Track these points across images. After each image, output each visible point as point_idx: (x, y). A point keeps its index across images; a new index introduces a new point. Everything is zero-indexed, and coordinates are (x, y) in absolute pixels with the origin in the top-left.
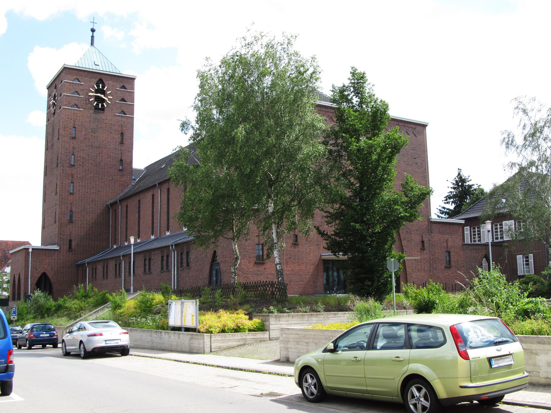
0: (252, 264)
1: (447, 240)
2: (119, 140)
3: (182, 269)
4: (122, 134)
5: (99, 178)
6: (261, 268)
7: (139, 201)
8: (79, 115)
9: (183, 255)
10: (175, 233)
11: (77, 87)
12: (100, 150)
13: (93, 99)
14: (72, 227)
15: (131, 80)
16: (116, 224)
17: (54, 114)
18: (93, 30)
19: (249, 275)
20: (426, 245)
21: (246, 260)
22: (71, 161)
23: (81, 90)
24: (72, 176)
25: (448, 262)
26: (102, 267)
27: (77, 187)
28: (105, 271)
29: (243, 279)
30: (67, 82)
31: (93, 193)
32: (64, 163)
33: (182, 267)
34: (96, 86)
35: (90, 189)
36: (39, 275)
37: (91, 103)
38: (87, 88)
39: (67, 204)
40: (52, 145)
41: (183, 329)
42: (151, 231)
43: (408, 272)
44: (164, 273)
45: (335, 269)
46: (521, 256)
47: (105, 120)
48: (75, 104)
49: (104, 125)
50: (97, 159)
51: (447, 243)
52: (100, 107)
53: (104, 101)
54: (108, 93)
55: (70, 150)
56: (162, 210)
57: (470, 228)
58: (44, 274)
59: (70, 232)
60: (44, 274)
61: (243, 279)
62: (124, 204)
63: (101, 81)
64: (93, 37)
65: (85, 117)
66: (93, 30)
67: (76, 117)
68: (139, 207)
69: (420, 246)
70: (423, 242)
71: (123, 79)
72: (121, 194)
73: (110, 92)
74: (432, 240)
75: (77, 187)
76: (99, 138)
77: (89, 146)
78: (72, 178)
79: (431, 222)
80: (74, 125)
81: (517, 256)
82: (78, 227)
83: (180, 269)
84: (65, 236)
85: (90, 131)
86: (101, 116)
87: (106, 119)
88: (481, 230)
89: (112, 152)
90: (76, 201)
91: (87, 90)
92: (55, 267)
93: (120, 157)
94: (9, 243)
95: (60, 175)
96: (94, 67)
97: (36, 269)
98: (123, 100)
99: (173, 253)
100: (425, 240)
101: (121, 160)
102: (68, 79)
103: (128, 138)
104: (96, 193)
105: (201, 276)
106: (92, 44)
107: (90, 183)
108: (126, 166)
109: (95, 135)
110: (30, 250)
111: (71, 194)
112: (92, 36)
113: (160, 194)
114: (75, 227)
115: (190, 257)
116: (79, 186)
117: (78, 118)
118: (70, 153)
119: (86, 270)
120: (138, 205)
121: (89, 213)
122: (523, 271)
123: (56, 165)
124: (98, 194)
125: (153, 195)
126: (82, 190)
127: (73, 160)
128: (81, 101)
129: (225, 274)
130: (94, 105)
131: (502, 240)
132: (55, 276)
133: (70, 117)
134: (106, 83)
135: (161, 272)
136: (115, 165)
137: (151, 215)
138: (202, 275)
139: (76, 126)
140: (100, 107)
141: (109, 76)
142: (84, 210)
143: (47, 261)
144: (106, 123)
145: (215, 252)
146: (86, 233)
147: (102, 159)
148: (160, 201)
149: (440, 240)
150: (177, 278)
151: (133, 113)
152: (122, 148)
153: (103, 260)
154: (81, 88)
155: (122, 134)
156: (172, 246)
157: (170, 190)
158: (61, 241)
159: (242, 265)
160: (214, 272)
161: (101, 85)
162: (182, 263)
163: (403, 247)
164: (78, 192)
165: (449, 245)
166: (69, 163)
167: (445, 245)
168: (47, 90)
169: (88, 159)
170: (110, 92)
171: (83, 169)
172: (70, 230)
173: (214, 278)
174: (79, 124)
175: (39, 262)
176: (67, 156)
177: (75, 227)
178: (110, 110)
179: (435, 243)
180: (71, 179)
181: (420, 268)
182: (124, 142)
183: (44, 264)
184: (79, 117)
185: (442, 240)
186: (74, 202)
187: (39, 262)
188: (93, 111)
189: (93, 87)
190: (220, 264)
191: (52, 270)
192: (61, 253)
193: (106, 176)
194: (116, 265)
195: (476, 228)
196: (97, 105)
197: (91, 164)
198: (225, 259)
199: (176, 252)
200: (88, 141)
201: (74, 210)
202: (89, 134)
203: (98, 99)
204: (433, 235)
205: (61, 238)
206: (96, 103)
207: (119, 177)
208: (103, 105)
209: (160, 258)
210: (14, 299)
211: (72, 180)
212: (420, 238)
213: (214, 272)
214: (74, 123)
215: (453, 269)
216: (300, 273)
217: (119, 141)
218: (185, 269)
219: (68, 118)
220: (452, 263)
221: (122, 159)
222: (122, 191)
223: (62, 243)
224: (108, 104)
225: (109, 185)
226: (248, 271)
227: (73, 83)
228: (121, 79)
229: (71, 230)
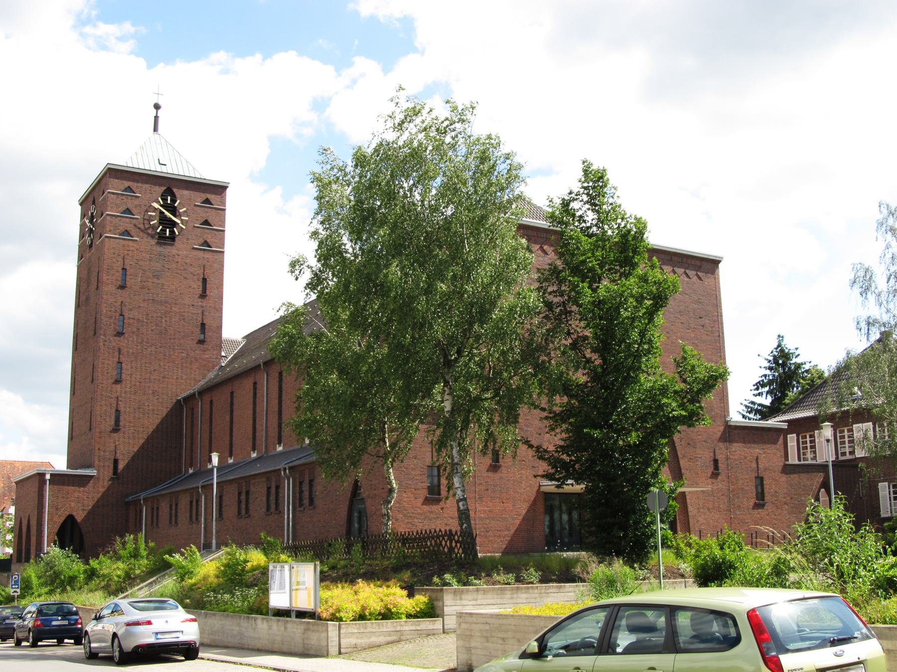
0: (421, 500)
3: (302, 509)
4: (204, 280)
6: (436, 508)
7: (232, 393)
8: (131, 249)
10: (292, 448)
11: (130, 201)
14: (119, 438)
15: (220, 189)
16: (192, 432)
17: (91, 246)
18: (157, 107)
19: (416, 520)
20: (721, 465)
23: (136, 206)
24: (120, 351)
25: (760, 495)
26: (169, 506)
28: (174, 512)
30: (113, 193)
31: (155, 379)
32: (105, 330)
33: (301, 505)
34: (162, 199)
36: (63, 519)
37: (154, 228)
40: (87, 299)
41: (293, 615)
42: (251, 444)
43: (690, 514)
45: (564, 508)
46: (886, 484)
49: (175, 266)
50: (161, 322)
53: (174, 224)
54: (181, 211)
57: (798, 436)
58: (71, 518)
59: (116, 447)
60: (71, 518)
62: (207, 398)
63: (169, 192)
64: (156, 118)
65: (141, 252)
66: (157, 107)
67: (127, 252)
68: (232, 404)
69: (711, 469)
70: (716, 461)
72: (202, 383)
73: (185, 209)
74: (731, 457)
76: (165, 287)
81: (880, 484)
83: (298, 509)
85: (151, 275)
88: (817, 440)
90: (126, 392)
91: (145, 206)
93: (200, 319)
94: (17, 465)
96: (159, 168)
99: (286, 481)
100: (718, 457)
101: (203, 325)
104: (159, 380)
105: (334, 522)
106: (155, 129)
108: (210, 334)
109: (160, 282)
110: (48, 477)
113: (267, 381)
115: (314, 489)
116: (132, 368)
117: (130, 253)
119: (141, 511)
120: (229, 400)
122: (889, 510)
123: (93, 332)
125: (255, 383)
129: (375, 517)
130: (158, 231)
135: (267, 515)
137: (251, 416)
138: (335, 520)
139: (127, 267)
140: (168, 235)
143: (76, 495)
148: (267, 394)
149: (745, 458)
151: (224, 245)
153: (171, 493)
155: (204, 280)
156: (285, 469)
159: (404, 501)
160: (356, 514)
161: (169, 198)
162: (301, 499)
163: (683, 471)
164: (128, 378)
167: (754, 465)
168: (80, 207)
169: (147, 323)
170: (185, 209)
171: (137, 339)
172: (114, 442)
173: (356, 525)
174: (131, 263)
177: (124, 437)
179: (738, 462)
181: (711, 507)
182: (208, 293)
184: (133, 251)
186: (123, 395)
187: (63, 497)
189: (158, 202)
192: (99, 481)
193: (177, 351)
194: (191, 502)
195: (808, 437)
196: (163, 231)
197: (152, 330)
198: (375, 492)
201: (122, 409)
203: (164, 221)
206: (161, 227)
207: (198, 352)
208: (172, 232)
209: (264, 491)
210: (19, 560)
211: (119, 358)
212: (712, 455)
213: (356, 514)
214: (124, 262)
216: (504, 516)
217: (201, 292)
219: (114, 254)
222: (204, 376)
226: (413, 513)
229: (117, 443)
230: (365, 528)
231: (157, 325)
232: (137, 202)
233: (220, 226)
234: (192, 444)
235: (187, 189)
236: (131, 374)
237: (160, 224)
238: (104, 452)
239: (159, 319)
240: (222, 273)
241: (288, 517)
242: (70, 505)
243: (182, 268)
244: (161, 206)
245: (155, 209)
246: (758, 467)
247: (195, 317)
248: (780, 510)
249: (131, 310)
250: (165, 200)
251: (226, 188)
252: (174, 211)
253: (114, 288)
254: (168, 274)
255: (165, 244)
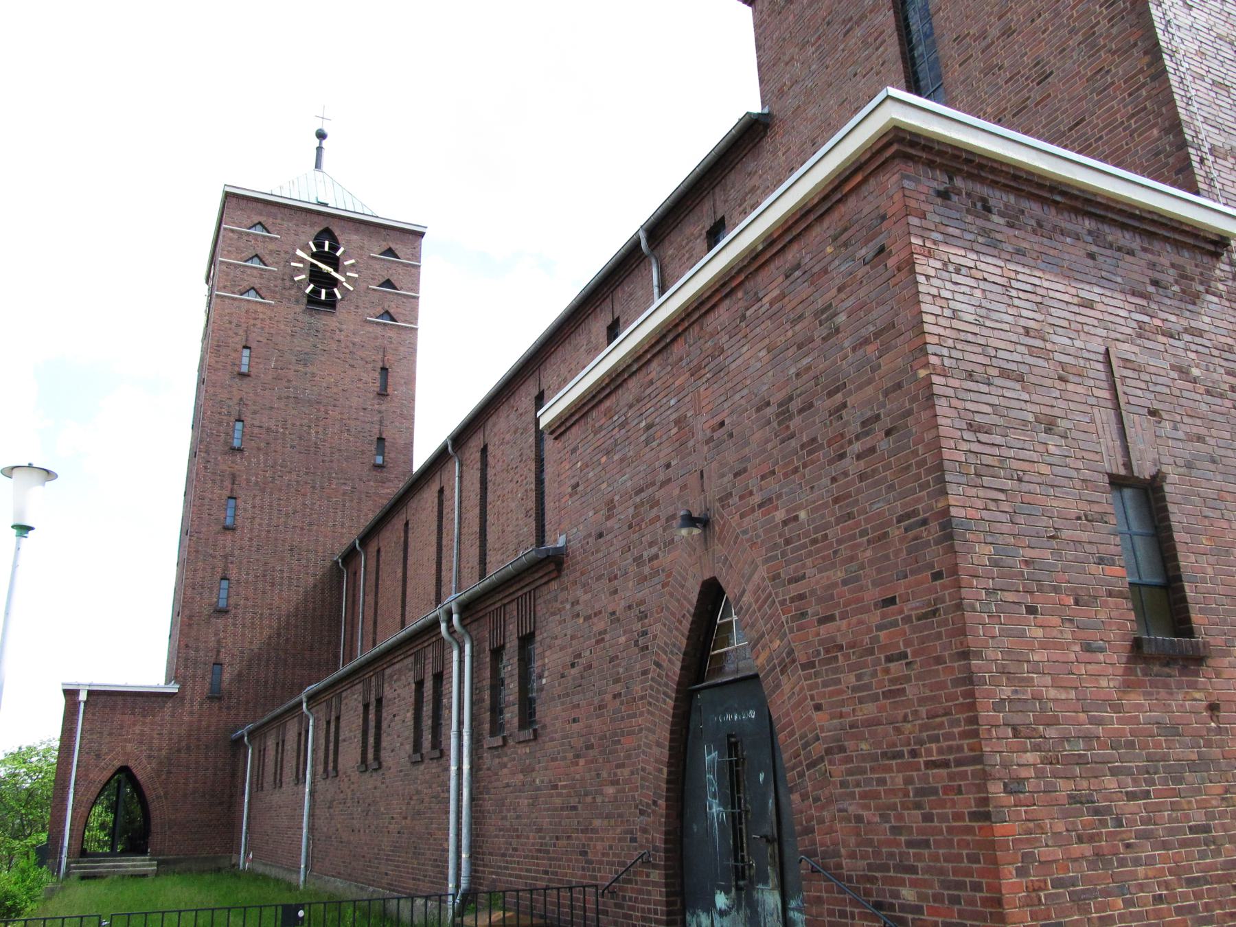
0: (1114, 659)
2: (376, 387)
3: (498, 741)
4: (384, 370)
5: (314, 487)
7: (407, 524)
8: (261, 316)
9: (505, 658)
11: (260, 244)
12: (318, 410)
13: (303, 277)
14: (226, 626)
18: (321, 135)
19: (1110, 783)
21: (1055, 620)
22: (233, 438)
23: (271, 252)
24: (234, 478)
27: (245, 509)
29: (1060, 826)
30: (232, 231)
31: (294, 527)
32: (209, 443)
35: (287, 515)
37: (300, 286)
38: (288, 248)
39: (215, 557)
44: (422, 767)
47: (338, 332)
48: (253, 288)
49: (334, 346)
50: (309, 434)
52: (323, 297)
53: (335, 282)
54: (346, 263)
55: (229, 406)
56: (464, 531)
59: (219, 641)
61: (1060, 826)
66: (321, 135)
67: (252, 322)
71: (389, 232)
73: (353, 261)
75: (245, 509)
77: (288, 397)
78: (233, 483)
80: (247, 340)
82: (244, 626)
83: (489, 741)
84: (202, 653)
85: (293, 359)
86: (325, 321)
87: (341, 331)
89: (354, 416)
90: (241, 549)
91: (287, 252)
92: (160, 750)
95: (197, 474)
97: (98, 756)
98: (388, 283)
101: (381, 440)
102: (234, 223)
103: (403, 381)
104: (302, 529)
105: (610, 790)
106: (318, 165)
107: (288, 499)
108: (392, 455)
110: (83, 696)
111: (226, 528)
112: (317, 148)
113: (461, 477)
114: (234, 625)
115: (536, 665)
116: (254, 507)
117: (258, 322)
118: (229, 414)
121: (281, 585)
124: (310, 531)
126: (261, 519)
127: (237, 434)
128: (269, 280)
129: (838, 770)
130: (308, 291)
132: (159, 776)
133: (235, 321)
134: (341, 239)
135: (415, 763)
136: (363, 452)
137: (434, 556)
138: (615, 783)
139: (253, 345)
140: (323, 297)
141: (351, 224)
142: (265, 576)
143: (137, 729)
144: (339, 341)
145: (712, 593)
146: (269, 644)
147: (325, 434)
150: (472, 799)
151: (416, 319)
152: (383, 408)
154: (272, 246)
155: (384, 370)
156: (449, 614)
157: (490, 448)
158: (186, 667)
159: (1036, 668)
160: (711, 757)
161: (327, 243)
162: (496, 709)
164: (247, 524)
166: (226, 443)
169: (284, 434)
171: (266, 460)
173: (715, 809)
174: (260, 339)
175: (110, 734)
176: (220, 423)
177: (234, 625)
178: (352, 308)
180: (230, 486)
182: (390, 390)
183: (125, 740)
186: (236, 553)
187: (110, 734)
188: (304, 307)
189: (305, 248)
190: (768, 684)
191: (149, 757)
192: (183, 705)
193: (335, 481)
196: (316, 292)
197: (293, 447)
198: (823, 630)
199: (467, 648)
200: (286, 384)
202: (290, 366)
205: (187, 659)
207: (372, 483)
208: (331, 295)
209: (408, 693)
211: (232, 490)
213: (711, 757)
214: (247, 337)
217: (377, 389)
218: (511, 742)
219: (230, 323)
221: (384, 436)
223: (190, 673)
224: (345, 291)
225: (344, 506)
226: (1088, 738)
227: (249, 234)
228: (384, 232)
229: (222, 635)
230: (769, 828)
231: (300, 438)
232: (272, 246)
233: (411, 290)
234: (352, 635)
235: (357, 231)
236: (254, 518)
237: (311, 281)
238: (197, 650)
239: (305, 428)
240: (414, 362)
241: (460, 769)
242: (124, 748)
243: (347, 351)
244: (313, 255)
245: (302, 260)
247: (368, 427)
249: (255, 412)
250: (319, 245)
251: (422, 235)
252: (335, 263)
253: (227, 377)
254: (323, 359)
255: (318, 312)
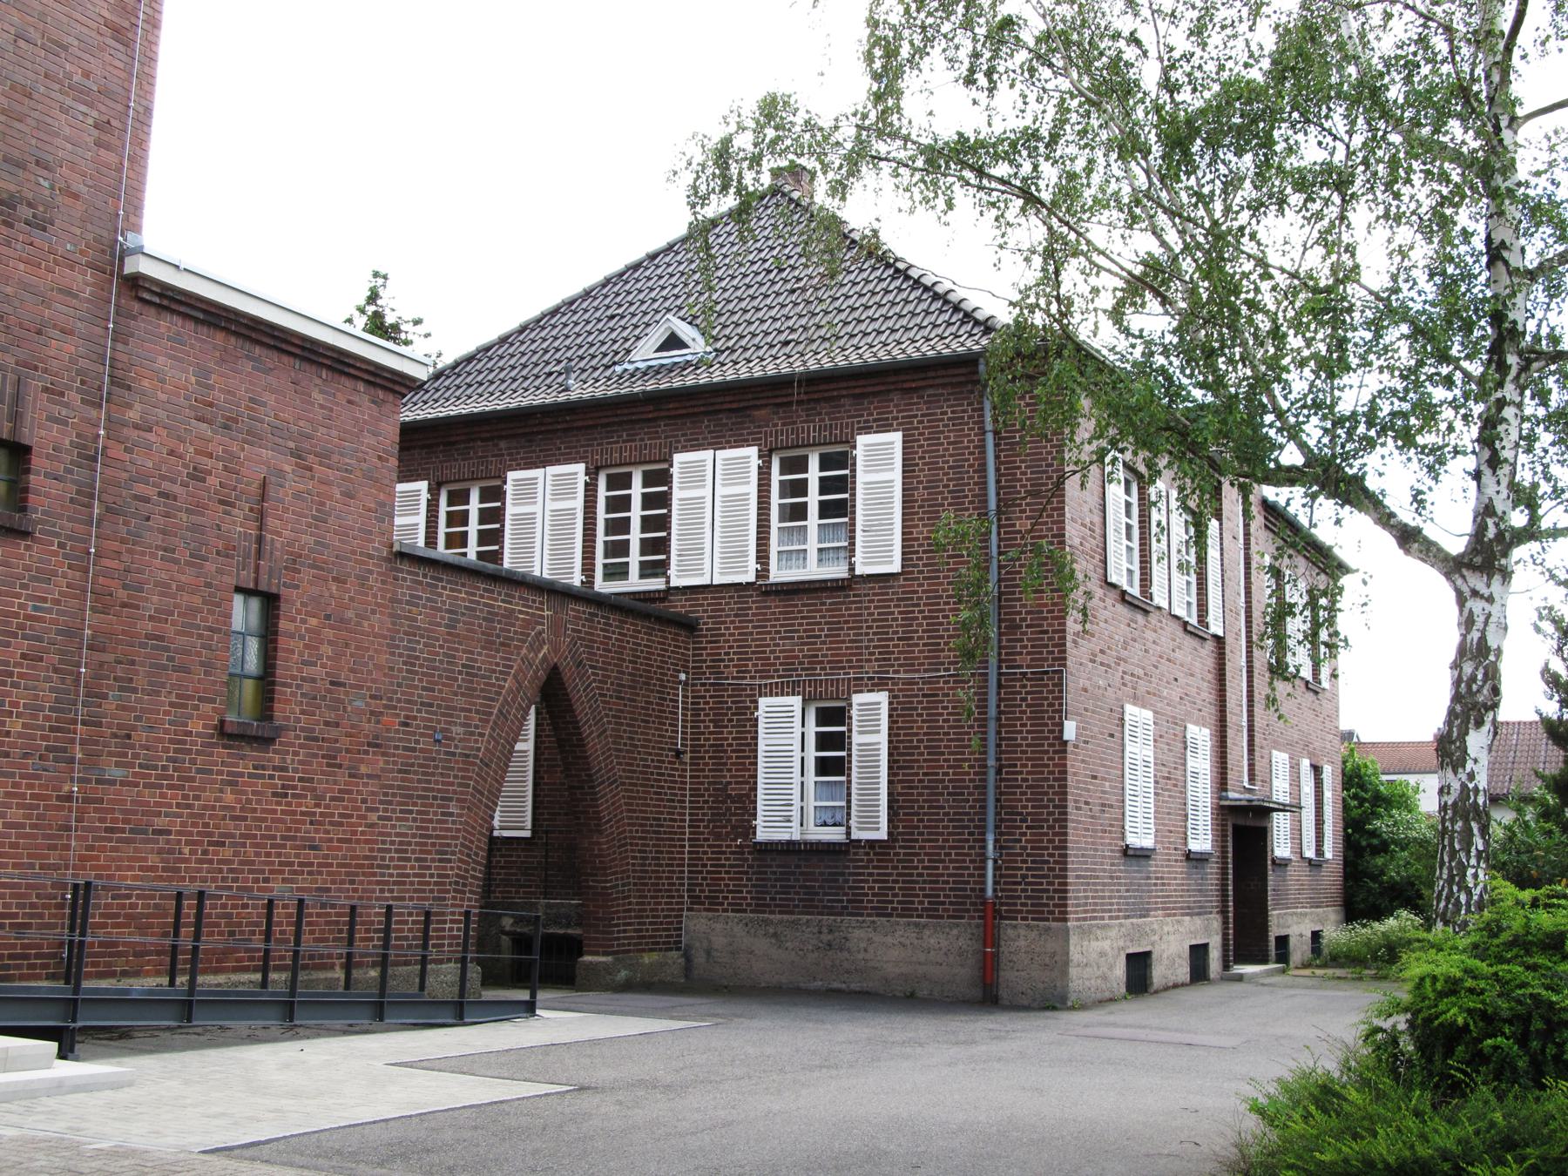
1: (264, 485)
25: (249, 687)
46: (796, 701)
51: (261, 517)
74: (117, 451)
79: (136, 283)
88: (511, 510)
122: (796, 814)
131: (657, 584)
149: (198, 475)
165: (281, 532)
167: (239, 525)
179: (151, 492)
185: (212, 481)
204: (133, 415)
215: (290, 755)
220: (288, 709)
246: (260, 540)
248: (342, 777)
